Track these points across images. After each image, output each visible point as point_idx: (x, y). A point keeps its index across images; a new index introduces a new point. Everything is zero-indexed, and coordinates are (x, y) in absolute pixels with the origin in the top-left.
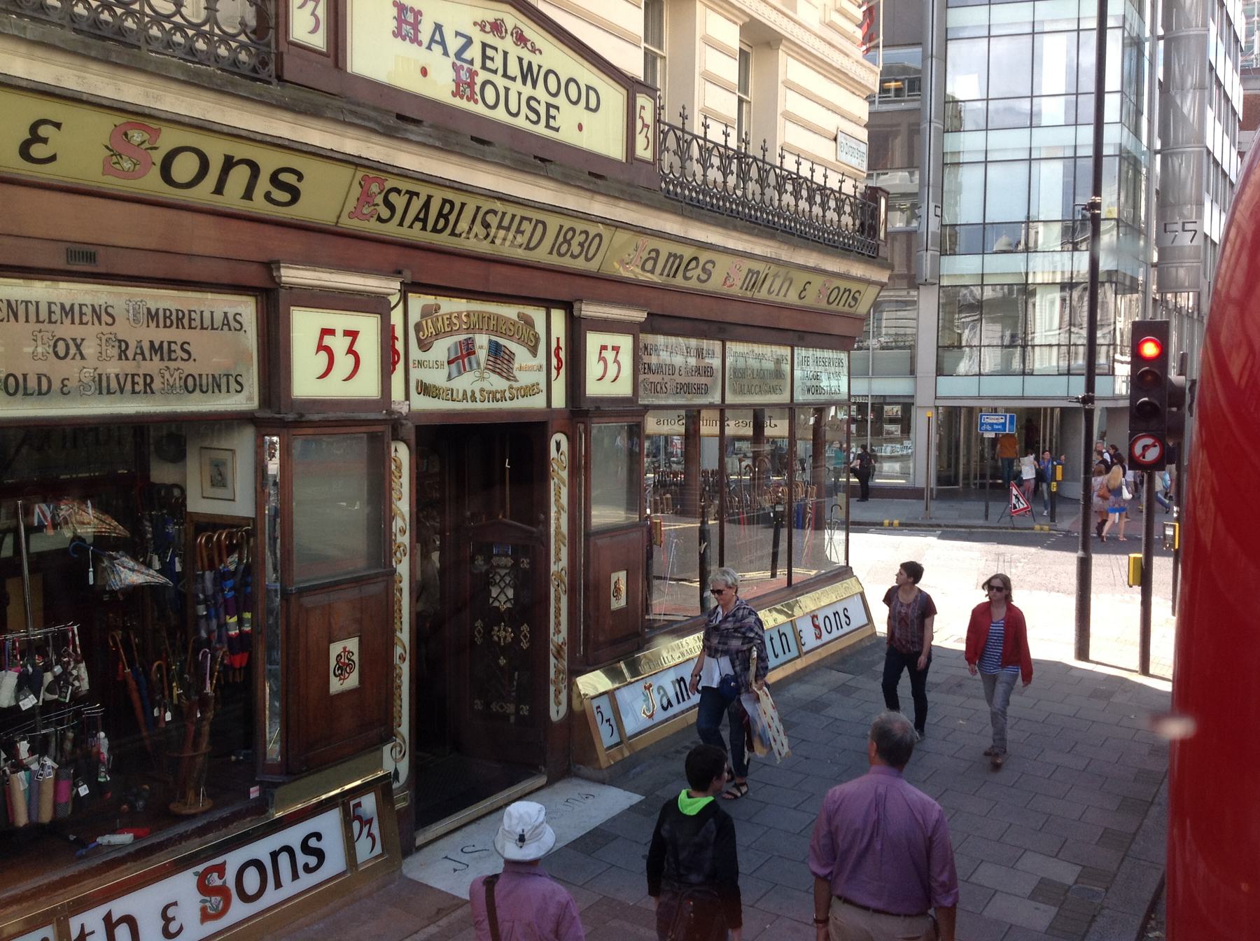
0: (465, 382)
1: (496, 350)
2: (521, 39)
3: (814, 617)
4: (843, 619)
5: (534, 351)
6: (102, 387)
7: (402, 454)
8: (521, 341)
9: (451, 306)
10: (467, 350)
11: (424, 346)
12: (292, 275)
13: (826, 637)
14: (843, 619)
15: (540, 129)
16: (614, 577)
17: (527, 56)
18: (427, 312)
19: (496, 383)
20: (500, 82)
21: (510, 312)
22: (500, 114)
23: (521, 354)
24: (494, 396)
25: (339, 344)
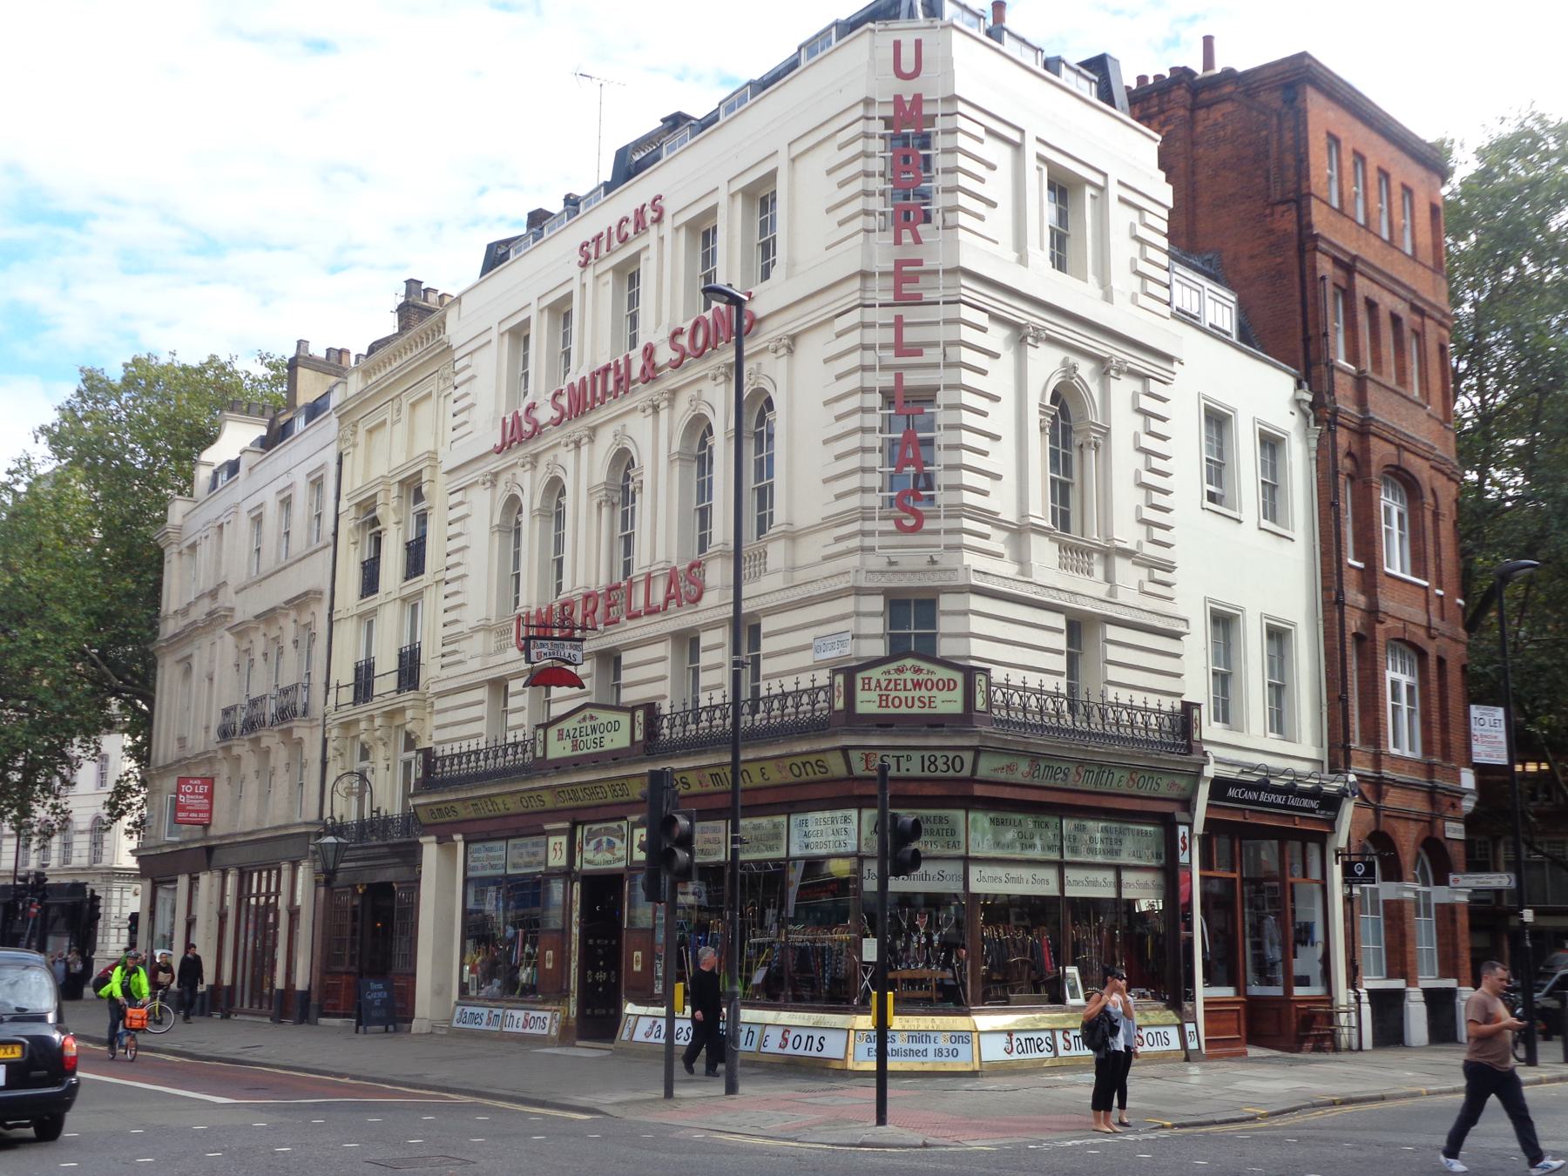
0: (599, 857)
1: (609, 842)
2: (592, 717)
3: (785, 1031)
4: (816, 1044)
5: (622, 840)
6: (527, 865)
7: (577, 886)
8: (617, 837)
9: (596, 827)
10: (599, 844)
11: (588, 844)
12: (547, 827)
13: (789, 1050)
14: (816, 1044)
15: (598, 749)
16: (636, 954)
17: (593, 723)
18: (590, 830)
19: (609, 856)
20: (584, 739)
21: (614, 825)
22: (585, 751)
23: (617, 841)
24: (608, 862)
25: (558, 847)
